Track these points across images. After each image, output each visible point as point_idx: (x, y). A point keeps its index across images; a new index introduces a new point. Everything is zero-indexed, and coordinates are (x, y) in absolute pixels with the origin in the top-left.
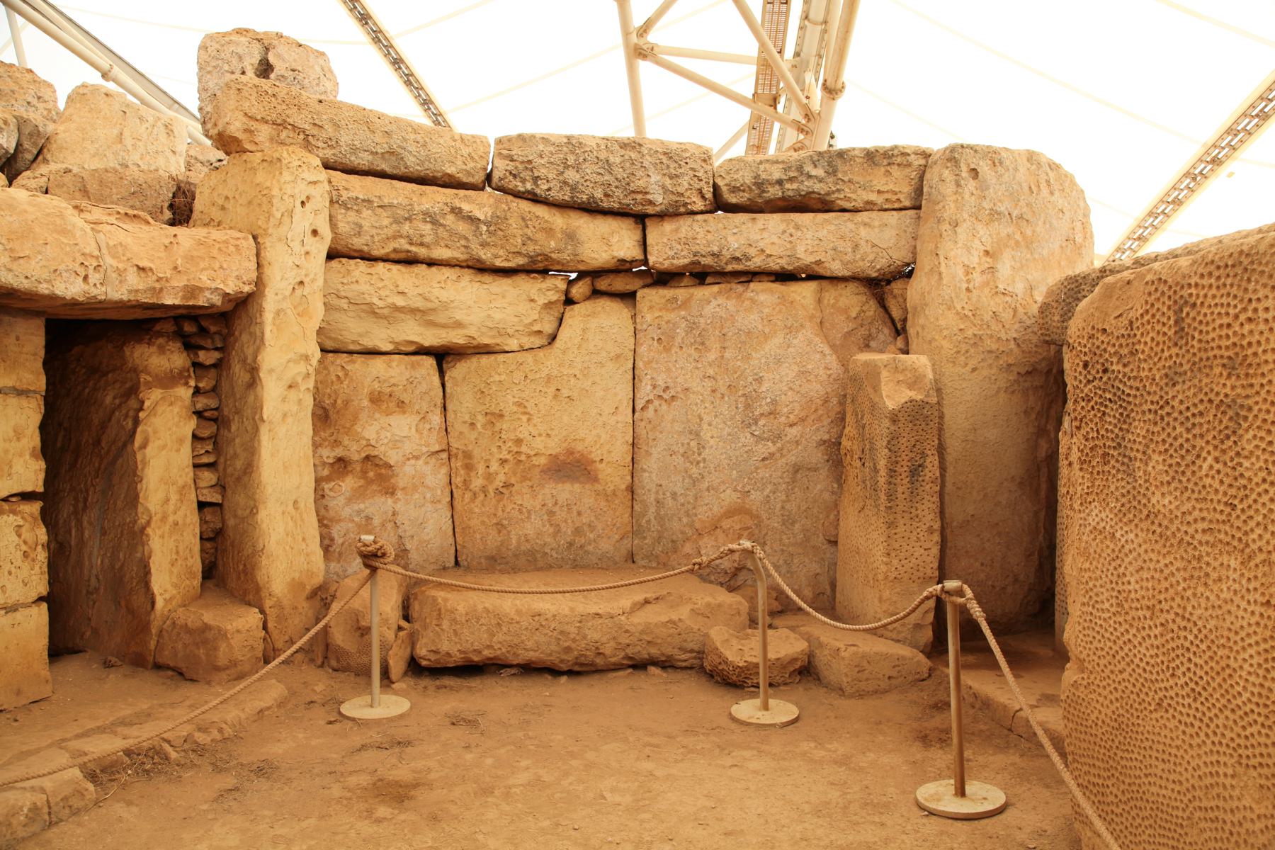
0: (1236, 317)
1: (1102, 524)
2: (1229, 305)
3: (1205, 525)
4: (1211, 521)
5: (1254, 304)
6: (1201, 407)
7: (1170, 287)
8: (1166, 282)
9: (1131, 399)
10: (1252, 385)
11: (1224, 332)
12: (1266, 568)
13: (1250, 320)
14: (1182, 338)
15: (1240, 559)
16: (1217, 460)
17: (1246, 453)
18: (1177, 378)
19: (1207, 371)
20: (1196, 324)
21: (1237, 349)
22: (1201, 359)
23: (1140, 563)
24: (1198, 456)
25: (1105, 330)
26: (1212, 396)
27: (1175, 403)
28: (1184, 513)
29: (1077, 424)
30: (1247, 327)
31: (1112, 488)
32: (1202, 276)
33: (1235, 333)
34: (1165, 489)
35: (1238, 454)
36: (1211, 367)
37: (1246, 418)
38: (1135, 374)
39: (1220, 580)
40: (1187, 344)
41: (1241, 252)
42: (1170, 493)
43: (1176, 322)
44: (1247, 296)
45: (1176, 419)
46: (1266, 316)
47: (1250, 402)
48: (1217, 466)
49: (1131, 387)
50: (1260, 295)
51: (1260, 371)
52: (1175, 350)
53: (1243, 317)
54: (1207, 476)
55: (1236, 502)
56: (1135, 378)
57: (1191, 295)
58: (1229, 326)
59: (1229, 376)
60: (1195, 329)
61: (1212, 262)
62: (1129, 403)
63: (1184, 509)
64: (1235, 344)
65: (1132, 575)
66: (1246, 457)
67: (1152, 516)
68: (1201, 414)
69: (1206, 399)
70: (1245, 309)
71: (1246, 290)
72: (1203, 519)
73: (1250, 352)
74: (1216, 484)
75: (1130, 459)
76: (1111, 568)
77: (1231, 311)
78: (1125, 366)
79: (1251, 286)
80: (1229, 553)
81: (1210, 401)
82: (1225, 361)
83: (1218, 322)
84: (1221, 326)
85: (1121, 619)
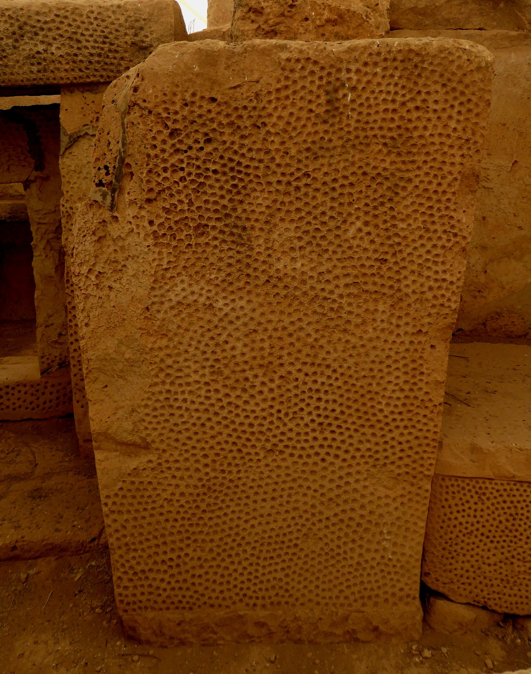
0: (403, 104)
1: (191, 298)
2: (396, 93)
3: (349, 280)
4: (356, 276)
5: (423, 96)
6: (352, 179)
7: (323, 68)
8: (316, 63)
9: (250, 171)
10: (413, 162)
11: (390, 115)
12: (418, 306)
13: (417, 108)
14: (334, 116)
15: (390, 302)
16: (366, 224)
17: (400, 216)
18: (320, 153)
19: (362, 147)
20: (355, 106)
21: (402, 131)
22: (357, 137)
23: (252, 326)
24: (345, 221)
25: (213, 100)
26: (368, 170)
27: (319, 175)
28: (321, 274)
29: (152, 196)
30: (415, 115)
31: (212, 259)
32: (366, 64)
33: (402, 118)
34: (297, 254)
35: (393, 217)
36: (368, 145)
37: (404, 188)
38: (258, 146)
39: (364, 323)
40: (340, 122)
41: (411, 51)
42: (303, 257)
43: (329, 102)
44: (417, 89)
45: (317, 190)
46: (435, 107)
47: (411, 175)
48: (366, 229)
49: (252, 159)
50: (433, 88)
51: (424, 151)
52: (321, 128)
53: (411, 105)
54: (354, 238)
55: (388, 257)
56: (259, 150)
57: (349, 79)
58: (394, 111)
59: (389, 153)
60: (353, 110)
61: (379, 54)
62: (248, 175)
63: (323, 269)
64: (399, 127)
65: (238, 339)
66: (402, 220)
67: (274, 281)
68: (351, 184)
69: (360, 172)
70: (412, 99)
71: (416, 83)
72: (348, 275)
73: (416, 134)
74: (366, 244)
75: (244, 228)
76: (206, 339)
77: (399, 98)
78: (243, 137)
79: (421, 82)
80: (376, 300)
81: (365, 174)
82: (388, 141)
83: (382, 107)
84: (386, 110)
85: (219, 386)
